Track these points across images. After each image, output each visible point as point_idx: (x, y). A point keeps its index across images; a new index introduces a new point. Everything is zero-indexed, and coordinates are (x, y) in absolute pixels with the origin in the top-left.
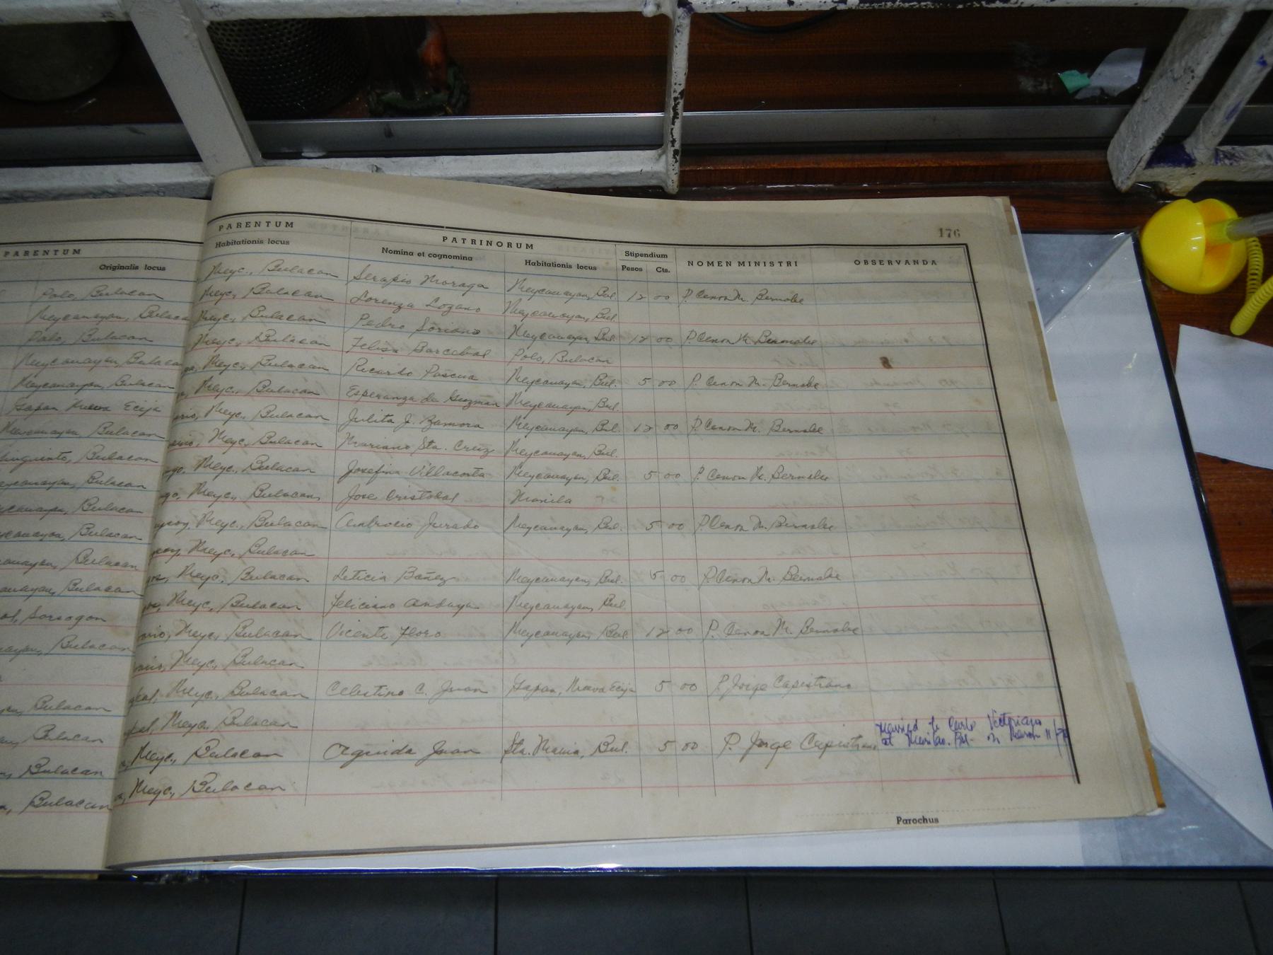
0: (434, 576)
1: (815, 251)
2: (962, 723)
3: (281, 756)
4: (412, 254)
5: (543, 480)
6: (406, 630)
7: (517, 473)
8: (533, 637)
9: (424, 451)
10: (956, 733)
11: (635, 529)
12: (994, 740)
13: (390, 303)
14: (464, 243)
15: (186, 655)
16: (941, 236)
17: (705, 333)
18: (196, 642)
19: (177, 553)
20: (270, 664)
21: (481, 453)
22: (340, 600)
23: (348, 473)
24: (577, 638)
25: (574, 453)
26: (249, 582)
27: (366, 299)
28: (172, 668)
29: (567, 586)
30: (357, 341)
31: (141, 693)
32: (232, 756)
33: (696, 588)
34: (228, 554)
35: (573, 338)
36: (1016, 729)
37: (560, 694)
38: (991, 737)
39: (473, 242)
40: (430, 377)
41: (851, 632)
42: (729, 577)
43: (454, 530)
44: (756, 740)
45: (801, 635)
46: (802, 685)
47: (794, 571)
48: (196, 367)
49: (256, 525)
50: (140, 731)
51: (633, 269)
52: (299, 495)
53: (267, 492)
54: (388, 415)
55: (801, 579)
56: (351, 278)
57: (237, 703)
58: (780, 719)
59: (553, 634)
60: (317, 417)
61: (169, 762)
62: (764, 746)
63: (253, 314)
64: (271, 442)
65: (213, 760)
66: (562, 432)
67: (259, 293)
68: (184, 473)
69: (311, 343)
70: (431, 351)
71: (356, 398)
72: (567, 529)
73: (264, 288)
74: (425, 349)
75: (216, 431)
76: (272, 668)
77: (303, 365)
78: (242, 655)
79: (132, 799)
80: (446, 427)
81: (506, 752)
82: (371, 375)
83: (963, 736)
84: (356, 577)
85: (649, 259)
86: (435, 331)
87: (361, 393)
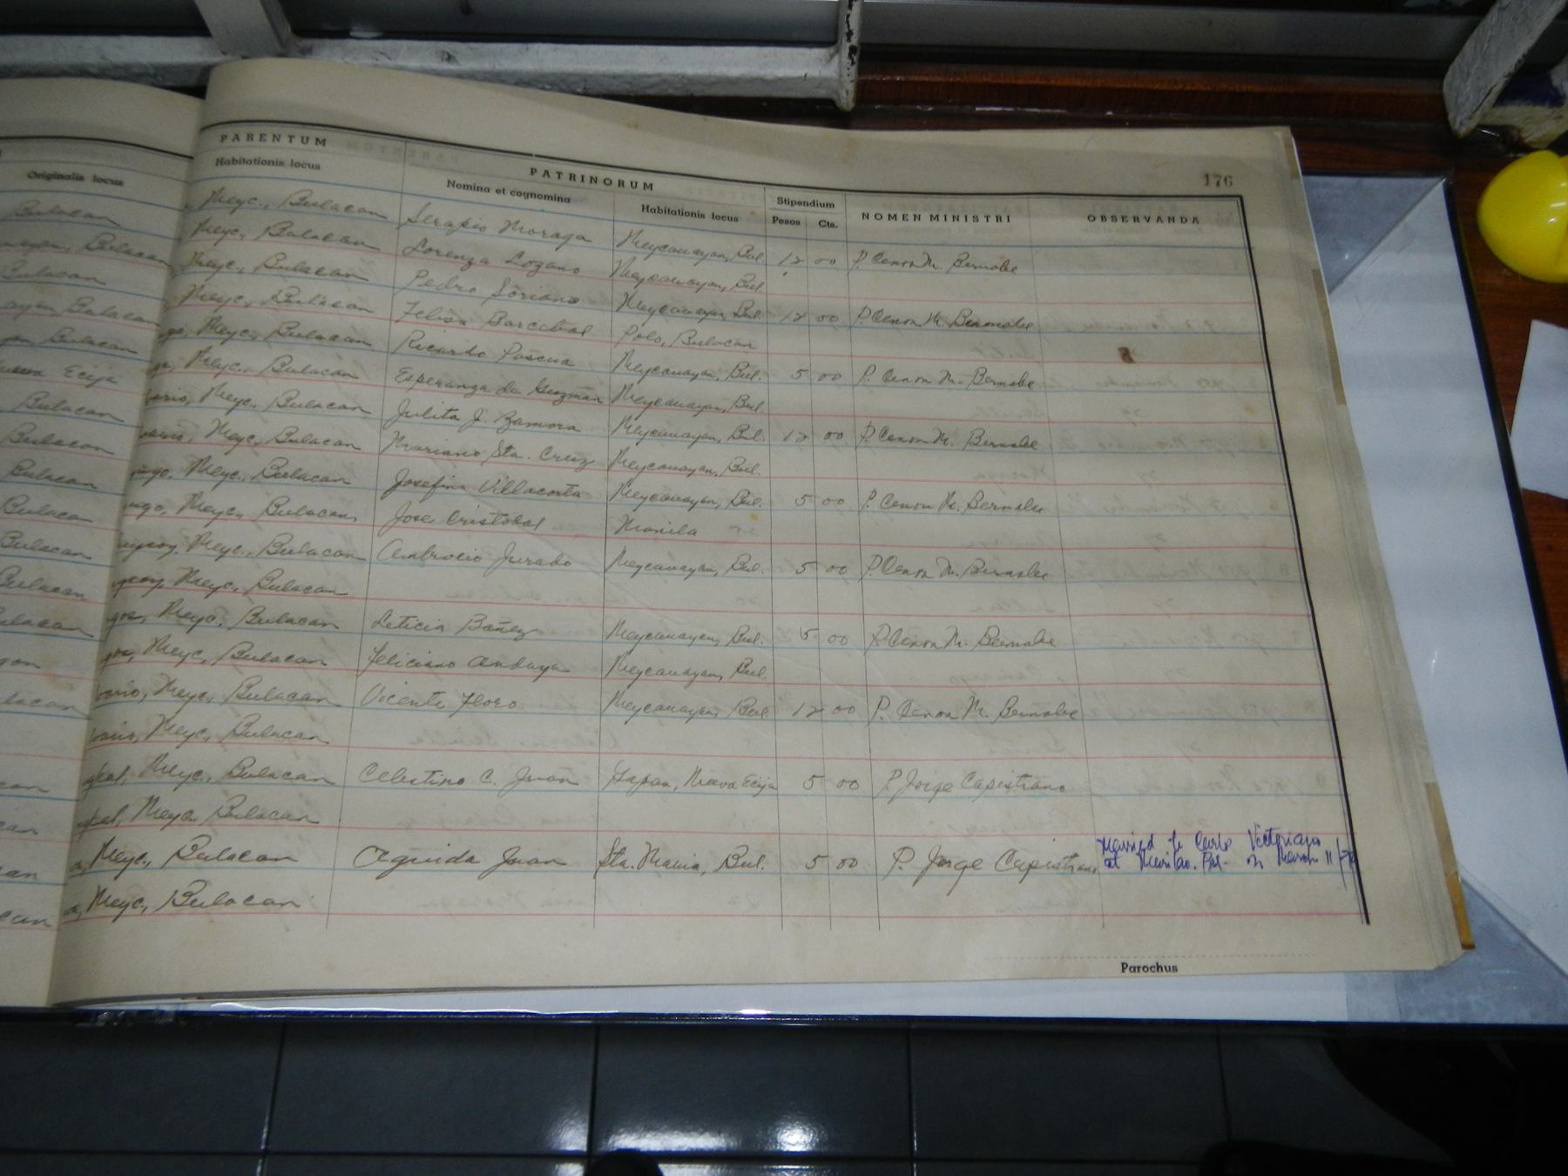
0: (508, 627)
1: (1035, 203)
2: (1213, 840)
3: (296, 861)
5: (659, 503)
6: (470, 697)
7: (624, 492)
8: (641, 712)
9: (500, 459)
10: (1205, 854)
11: (782, 571)
12: (1256, 864)
13: (456, 257)
14: (559, 177)
15: (168, 721)
16: (1207, 184)
17: (882, 310)
18: (180, 705)
19: (159, 584)
20: (283, 736)
21: (577, 464)
22: (380, 655)
24: (700, 716)
25: (703, 469)
26: (257, 626)
27: (425, 249)
28: (148, 737)
29: (689, 645)
30: (409, 307)
31: (104, 770)
32: (228, 859)
33: (860, 653)
34: (229, 588)
35: (705, 312)
36: (1285, 851)
37: (676, 788)
38: (1252, 860)
39: (572, 177)
40: (508, 359)
41: (1068, 717)
42: (906, 639)
43: (538, 567)
44: (935, 859)
45: (1000, 719)
46: (999, 786)
47: (993, 632)
48: (186, 329)
49: (268, 553)
50: (104, 822)
51: (787, 222)
52: (328, 513)
53: (285, 509)
54: (451, 410)
55: (1002, 644)
56: (404, 219)
57: (236, 788)
58: (968, 830)
59: (668, 708)
60: (354, 408)
61: (141, 864)
62: (946, 866)
63: (269, 264)
64: (291, 441)
65: (200, 863)
66: (686, 439)
67: (277, 235)
68: (170, 477)
69: (348, 307)
70: (511, 324)
72: (690, 570)
73: (284, 229)
74: (503, 321)
75: (216, 425)
76: (286, 741)
77: (337, 336)
78: (245, 723)
79: (90, 914)
80: (530, 428)
81: (601, 864)
82: (429, 353)
83: (1214, 857)
85: (809, 208)
87: (416, 377)
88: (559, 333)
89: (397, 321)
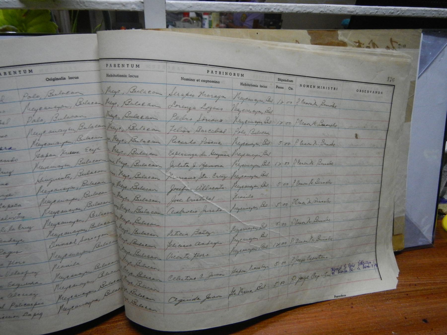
0: (205, 232)
4: (194, 80)
6: (196, 254)
9: (202, 179)
14: (216, 74)
22: (171, 244)
23: (171, 191)
40: (203, 144)
52: (152, 201)
54: (186, 163)
56: (168, 95)
64: (139, 177)
69: (152, 130)
71: (173, 156)
73: (130, 102)
74: (201, 130)
77: (149, 141)
80: (209, 168)
84: (176, 234)
86: (205, 121)
87: (175, 153)
88: (217, 133)
89: (168, 133)
